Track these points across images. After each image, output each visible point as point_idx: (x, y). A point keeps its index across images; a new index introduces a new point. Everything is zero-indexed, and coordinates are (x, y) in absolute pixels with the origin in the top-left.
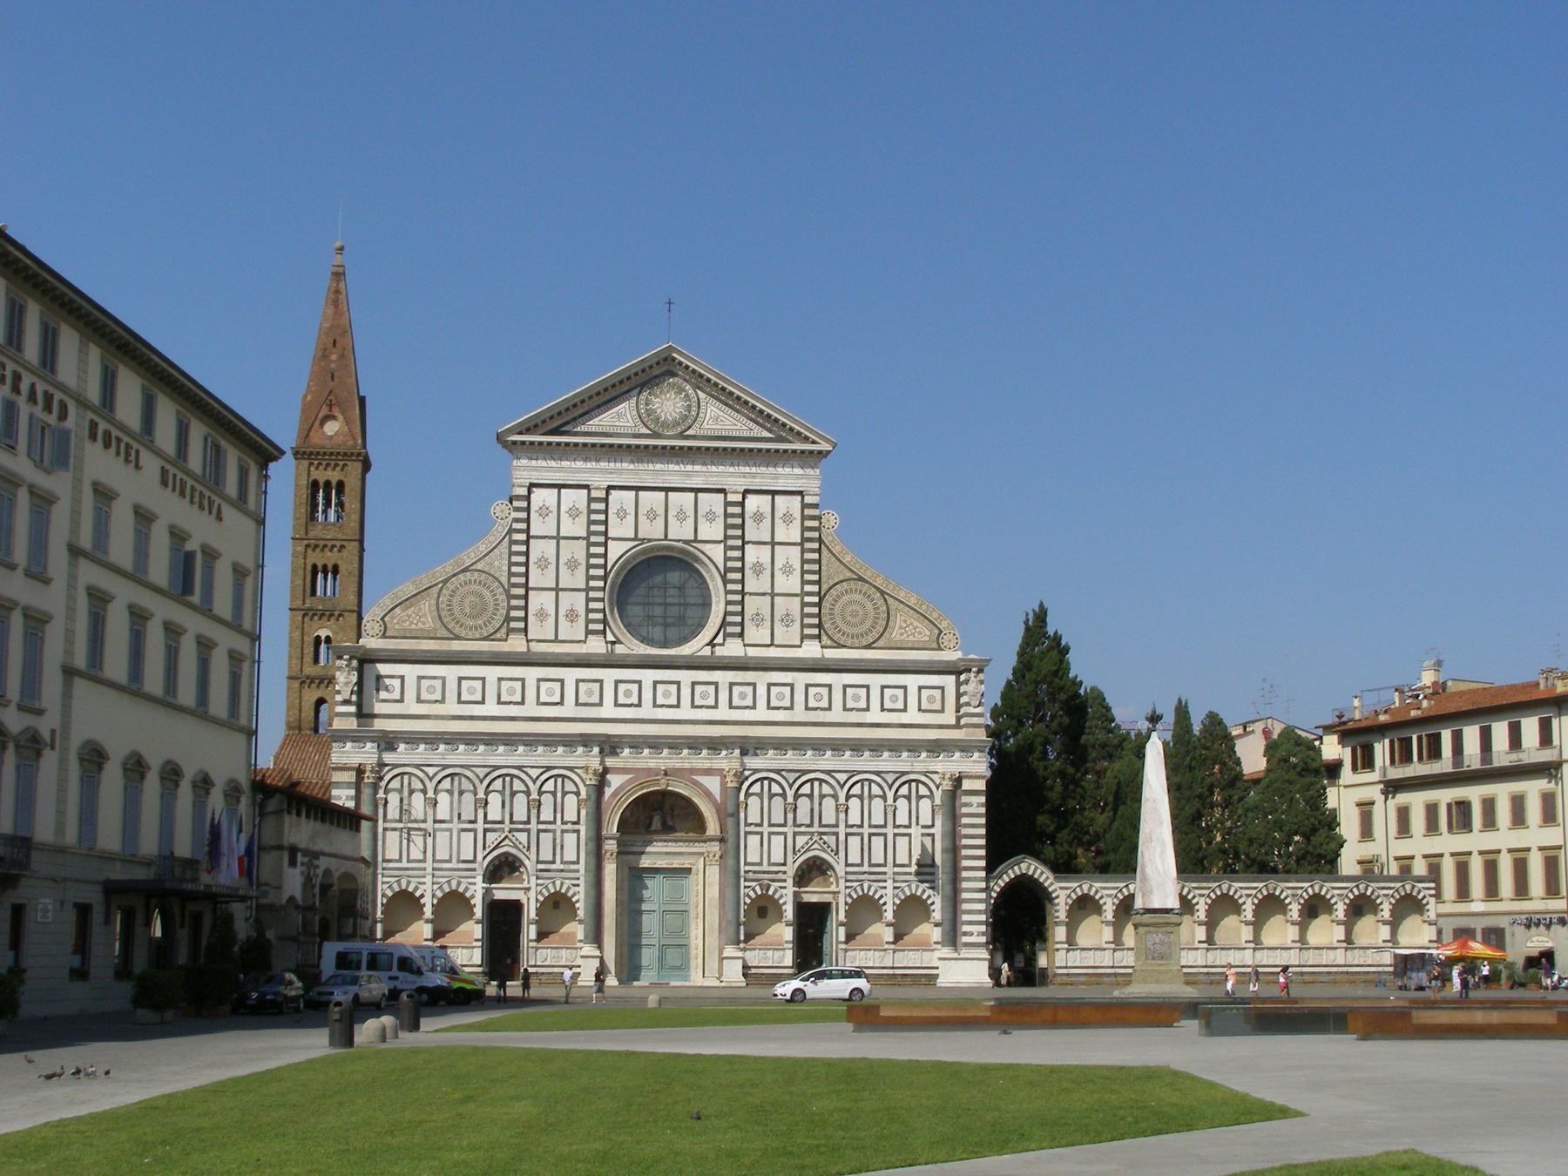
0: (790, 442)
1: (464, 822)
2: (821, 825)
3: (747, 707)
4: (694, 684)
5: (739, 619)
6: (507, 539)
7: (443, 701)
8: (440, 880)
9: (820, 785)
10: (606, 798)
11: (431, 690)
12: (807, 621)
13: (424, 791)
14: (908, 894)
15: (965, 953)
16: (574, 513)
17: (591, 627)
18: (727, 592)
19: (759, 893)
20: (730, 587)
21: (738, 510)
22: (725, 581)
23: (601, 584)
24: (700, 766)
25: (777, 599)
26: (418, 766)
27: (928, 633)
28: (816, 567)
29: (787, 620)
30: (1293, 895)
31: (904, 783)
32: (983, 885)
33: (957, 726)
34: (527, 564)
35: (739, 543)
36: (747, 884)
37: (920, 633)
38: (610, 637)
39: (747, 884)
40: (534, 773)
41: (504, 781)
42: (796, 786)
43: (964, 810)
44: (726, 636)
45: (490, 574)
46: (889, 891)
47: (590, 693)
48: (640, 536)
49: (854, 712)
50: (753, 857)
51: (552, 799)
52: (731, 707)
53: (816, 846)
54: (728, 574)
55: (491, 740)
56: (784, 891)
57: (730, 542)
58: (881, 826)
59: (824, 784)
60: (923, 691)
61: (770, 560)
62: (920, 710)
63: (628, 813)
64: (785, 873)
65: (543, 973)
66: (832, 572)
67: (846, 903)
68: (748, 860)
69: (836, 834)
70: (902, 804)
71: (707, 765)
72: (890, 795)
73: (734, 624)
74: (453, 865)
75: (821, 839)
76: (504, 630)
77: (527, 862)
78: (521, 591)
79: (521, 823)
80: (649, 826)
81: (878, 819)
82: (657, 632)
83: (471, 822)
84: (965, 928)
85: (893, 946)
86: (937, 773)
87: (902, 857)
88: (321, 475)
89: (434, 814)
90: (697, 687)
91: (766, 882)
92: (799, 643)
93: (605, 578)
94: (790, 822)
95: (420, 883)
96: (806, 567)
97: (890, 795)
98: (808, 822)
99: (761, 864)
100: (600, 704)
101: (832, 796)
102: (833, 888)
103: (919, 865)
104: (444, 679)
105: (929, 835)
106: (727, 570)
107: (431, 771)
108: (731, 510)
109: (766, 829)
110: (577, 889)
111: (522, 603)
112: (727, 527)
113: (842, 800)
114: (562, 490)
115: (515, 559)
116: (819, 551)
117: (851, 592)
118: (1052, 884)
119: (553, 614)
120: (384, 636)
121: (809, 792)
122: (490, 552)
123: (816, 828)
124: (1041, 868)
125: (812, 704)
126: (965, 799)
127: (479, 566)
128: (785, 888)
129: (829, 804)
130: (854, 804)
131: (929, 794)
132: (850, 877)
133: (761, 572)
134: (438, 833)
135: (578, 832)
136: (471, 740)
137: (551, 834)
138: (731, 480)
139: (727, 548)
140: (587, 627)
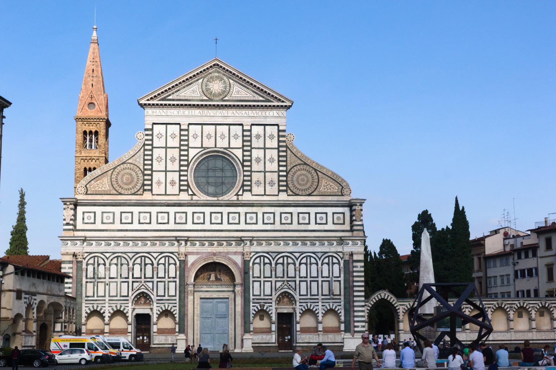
0: (272, 102)
1: (123, 278)
2: (288, 277)
4: (229, 213)
5: (249, 183)
6: (143, 149)
7: (113, 223)
8: (112, 305)
9: (287, 259)
10: (189, 266)
11: (108, 218)
12: (281, 183)
13: (105, 264)
14: (329, 308)
15: (356, 335)
16: (173, 136)
17: (182, 188)
18: (244, 171)
19: (260, 308)
20: (245, 168)
21: (248, 133)
22: (243, 166)
23: (186, 168)
24: (232, 251)
25: (267, 173)
26: (102, 253)
27: (337, 188)
28: (284, 159)
30: (511, 307)
31: (326, 257)
32: (363, 304)
33: (352, 230)
34: (152, 160)
35: (249, 148)
36: (254, 305)
39: (254, 305)
40: (155, 255)
41: (141, 259)
43: (355, 269)
44: (244, 191)
45: (135, 165)
46: (320, 307)
47: (181, 218)
48: (204, 146)
49: (303, 225)
52: (246, 223)
53: (286, 287)
54: (244, 163)
55: (135, 240)
56: (271, 308)
57: (245, 148)
58: (315, 277)
59: (289, 259)
60: (335, 215)
62: (333, 223)
64: (271, 299)
65: (159, 348)
67: (300, 313)
68: (254, 294)
69: (295, 281)
70: (325, 267)
71: (235, 250)
72: (320, 263)
73: (247, 186)
74: (118, 298)
77: (152, 296)
78: (149, 172)
79: (149, 278)
80: (210, 278)
82: (211, 189)
83: (126, 278)
84: (356, 324)
85: (322, 333)
87: (326, 292)
88: (88, 128)
89: (109, 274)
90: (230, 215)
91: (262, 304)
92: (277, 194)
93: (188, 166)
94: (273, 276)
95: (103, 307)
96: (280, 159)
97: (320, 263)
98: (282, 276)
100: (186, 223)
102: (294, 306)
104: (114, 213)
105: (338, 281)
106: (244, 161)
108: (245, 133)
109: (262, 279)
110: (175, 308)
111: (150, 177)
112: (244, 141)
113: (297, 265)
114: (168, 126)
115: (146, 157)
117: (301, 170)
118: (396, 303)
120: (86, 194)
124: (391, 296)
125: (283, 221)
126: (355, 264)
127: (130, 161)
128: (271, 306)
129: (291, 267)
130: (303, 267)
131: (338, 262)
132: (302, 301)
133: (259, 162)
134: (111, 284)
135: (175, 282)
136: (126, 240)
137: (163, 283)
139: (244, 151)
140: (180, 188)
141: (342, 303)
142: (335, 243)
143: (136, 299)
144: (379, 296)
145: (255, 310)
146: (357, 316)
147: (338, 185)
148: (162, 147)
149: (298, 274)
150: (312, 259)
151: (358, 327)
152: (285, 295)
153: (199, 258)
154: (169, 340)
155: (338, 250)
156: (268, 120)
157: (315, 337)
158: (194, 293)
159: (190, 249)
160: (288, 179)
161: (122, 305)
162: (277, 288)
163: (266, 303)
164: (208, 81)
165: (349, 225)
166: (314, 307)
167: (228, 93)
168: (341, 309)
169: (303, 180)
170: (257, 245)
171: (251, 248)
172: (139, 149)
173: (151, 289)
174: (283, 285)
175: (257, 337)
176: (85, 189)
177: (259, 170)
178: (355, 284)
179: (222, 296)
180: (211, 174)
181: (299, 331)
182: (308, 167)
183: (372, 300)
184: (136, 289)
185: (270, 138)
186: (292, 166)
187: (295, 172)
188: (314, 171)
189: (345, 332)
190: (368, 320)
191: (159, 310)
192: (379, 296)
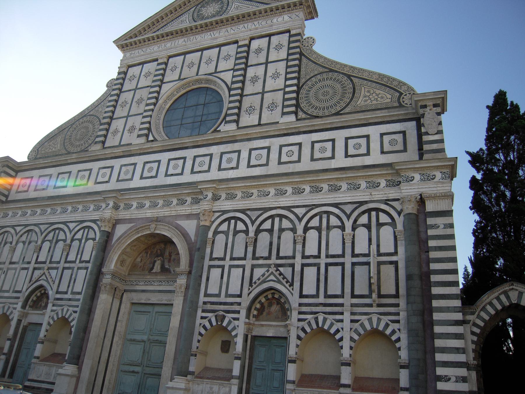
2: (278, 257)
3: (232, 168)
9: (281, 221)
13: (11, 243)
19: (214, 323)
22: (230, 90)
23: (152, 107)
24: (183, 213)
26: (13, 227)
27: (390, 96)
29: (272, 107)
31: (363, 213)
32: (459, 316)
36: (204, 315)
37: (382, 98)
38: (151, 138)
39: (204, 315)
41: (54, 234)
42: (258, 223)
43: (430, 232)
45: (95, 116)
46: (347, 324)
48: (181, 78)
49: (321, 161)
50: (213, 289)
51: (79, 244)
53: (272, 277)
56: (236, 323)
59: (284, 219)
61: (263, 73)
62: (382, 152)
63: (139, 260)
64: (239, 304)
66: (308, 69)
67: (299, 338)
68: (209, 292)
69: (293, 266)
70: (362, 233)
72: (348, 225)
75: (276, 271)
76: (93, 144)
77: (50, 293)
80: (152, 268)
81: (336, 248)
84: (440, 371)
85: (348, 390)
86: (398, 200)
87: (361, 288)
91: (221, 313)
93: (155, 104)
97: (348, 225)
98: (266, 254)
99: (218, 295)
103: (380, 296)
105: (391, 263)
107: (18, 229)
116: (300, 60)
119: (121, 130)
121: (270, 228)
122: (99, 105)
123: (274, 260)
125: (284, 159)
126: (430, 221)
127: (91, 113)
128: (237, 319)
129: (287, 236)
130: (312, 235)
131: (390, 221)
132: (304, 309)
138: (241, 35)
141: (403, 315)
142: (383, 183)
143: (35, 299)
144: (503, 298)
145: (204, 327)
146: (444, 350)
148: (130, 90)
149: (301, 249)
150: (332, 219)
151: (447, 379)
152: (273, 297)
153: (131, 228)
154: (51, 375)
155: (390, 195)
156: (274, 27)
158: (123, 294)
159: (123, 214)
160: (300, 96)
161: (11, 306)
162: (253, 281)
163: (228, 312)
164: (201, 7)
165: (417, 152)
166: (332, 325)
167: (225, 11)
168: (399, 330)
169: (325, 94)
170: (227, 199)
171: (214, 205)
172: (105, 97)
173: (53, 281)
174: (267, 274)
175: (201, 387)
176: (36, 153)
177: (254, 92)
178: (433, 266)
179: (166, 300)
180: (189, 113)
182: (336, 74)
183: (484, 309)
184: (34, 281)
185: (276, 49)
186: (308, 77)
187: (313, 85)
188: (346, 78)
190: (475, 362)
191: (53, 318)
192: (503, 298)
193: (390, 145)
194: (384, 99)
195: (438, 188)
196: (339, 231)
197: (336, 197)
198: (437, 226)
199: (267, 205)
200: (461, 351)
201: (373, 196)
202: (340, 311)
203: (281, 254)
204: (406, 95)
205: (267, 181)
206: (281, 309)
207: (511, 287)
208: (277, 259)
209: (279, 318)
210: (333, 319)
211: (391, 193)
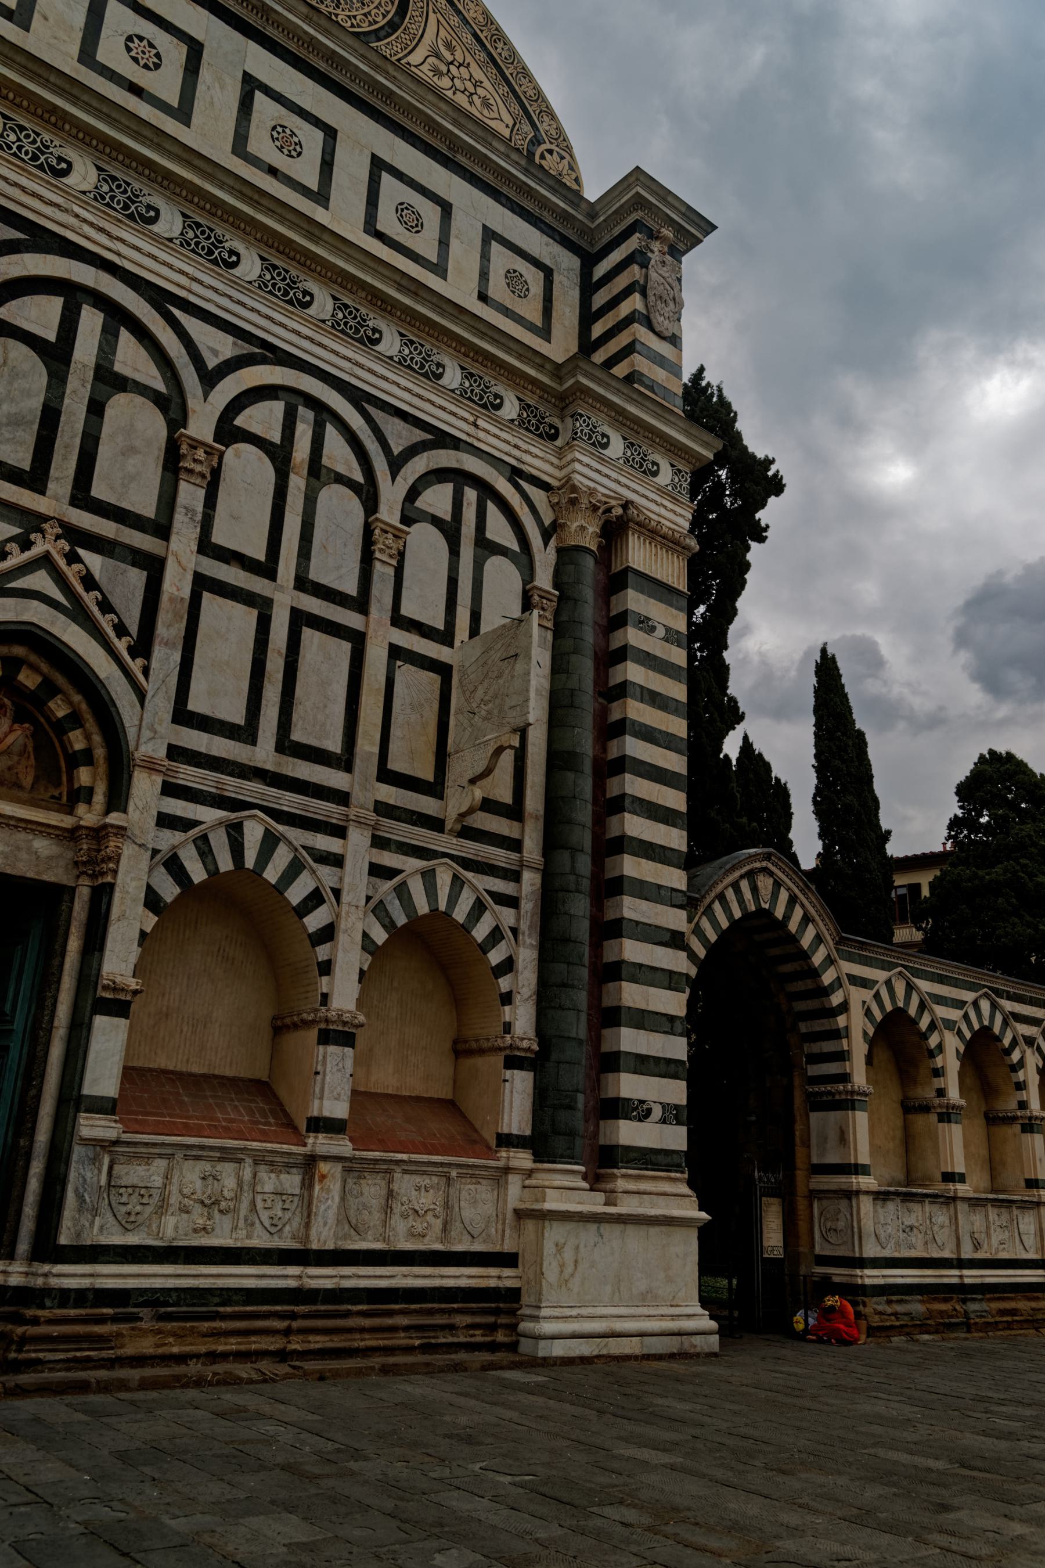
31: (440, 475)
32: (676, 919)
37: (486, 103)
53: (40, 581)
59: (125, 335)
67: (152, 901)
75: (72, 558)
85: (343, 1146)
86: (545, 487)
101: (159, 401)
118: (829, 961)
132: (189, 775)
144: (744, 885)
147: (516, 108)
157: (269, 1182)
166: (295, 869)
168: (515, 931)
174: (17, 558)
181: (104, 1107)
189: (539, 1157)
193: (508, 284)
194: (492, 115)
195: (663, 511)
196: (355, 506)
197: (361, 366)
198: (650, 623)
199: (51, 220)
200: (679, 1027)
201: (481, 435)
202: (334, 821)
203: (99, 490)
204: (550, 152)
205: (74, 104)
206: (35, 749)
207: (764, 864)
208: (74, 502)
209: (20, 787)
210: (304, 847)
211: (531, 453)
